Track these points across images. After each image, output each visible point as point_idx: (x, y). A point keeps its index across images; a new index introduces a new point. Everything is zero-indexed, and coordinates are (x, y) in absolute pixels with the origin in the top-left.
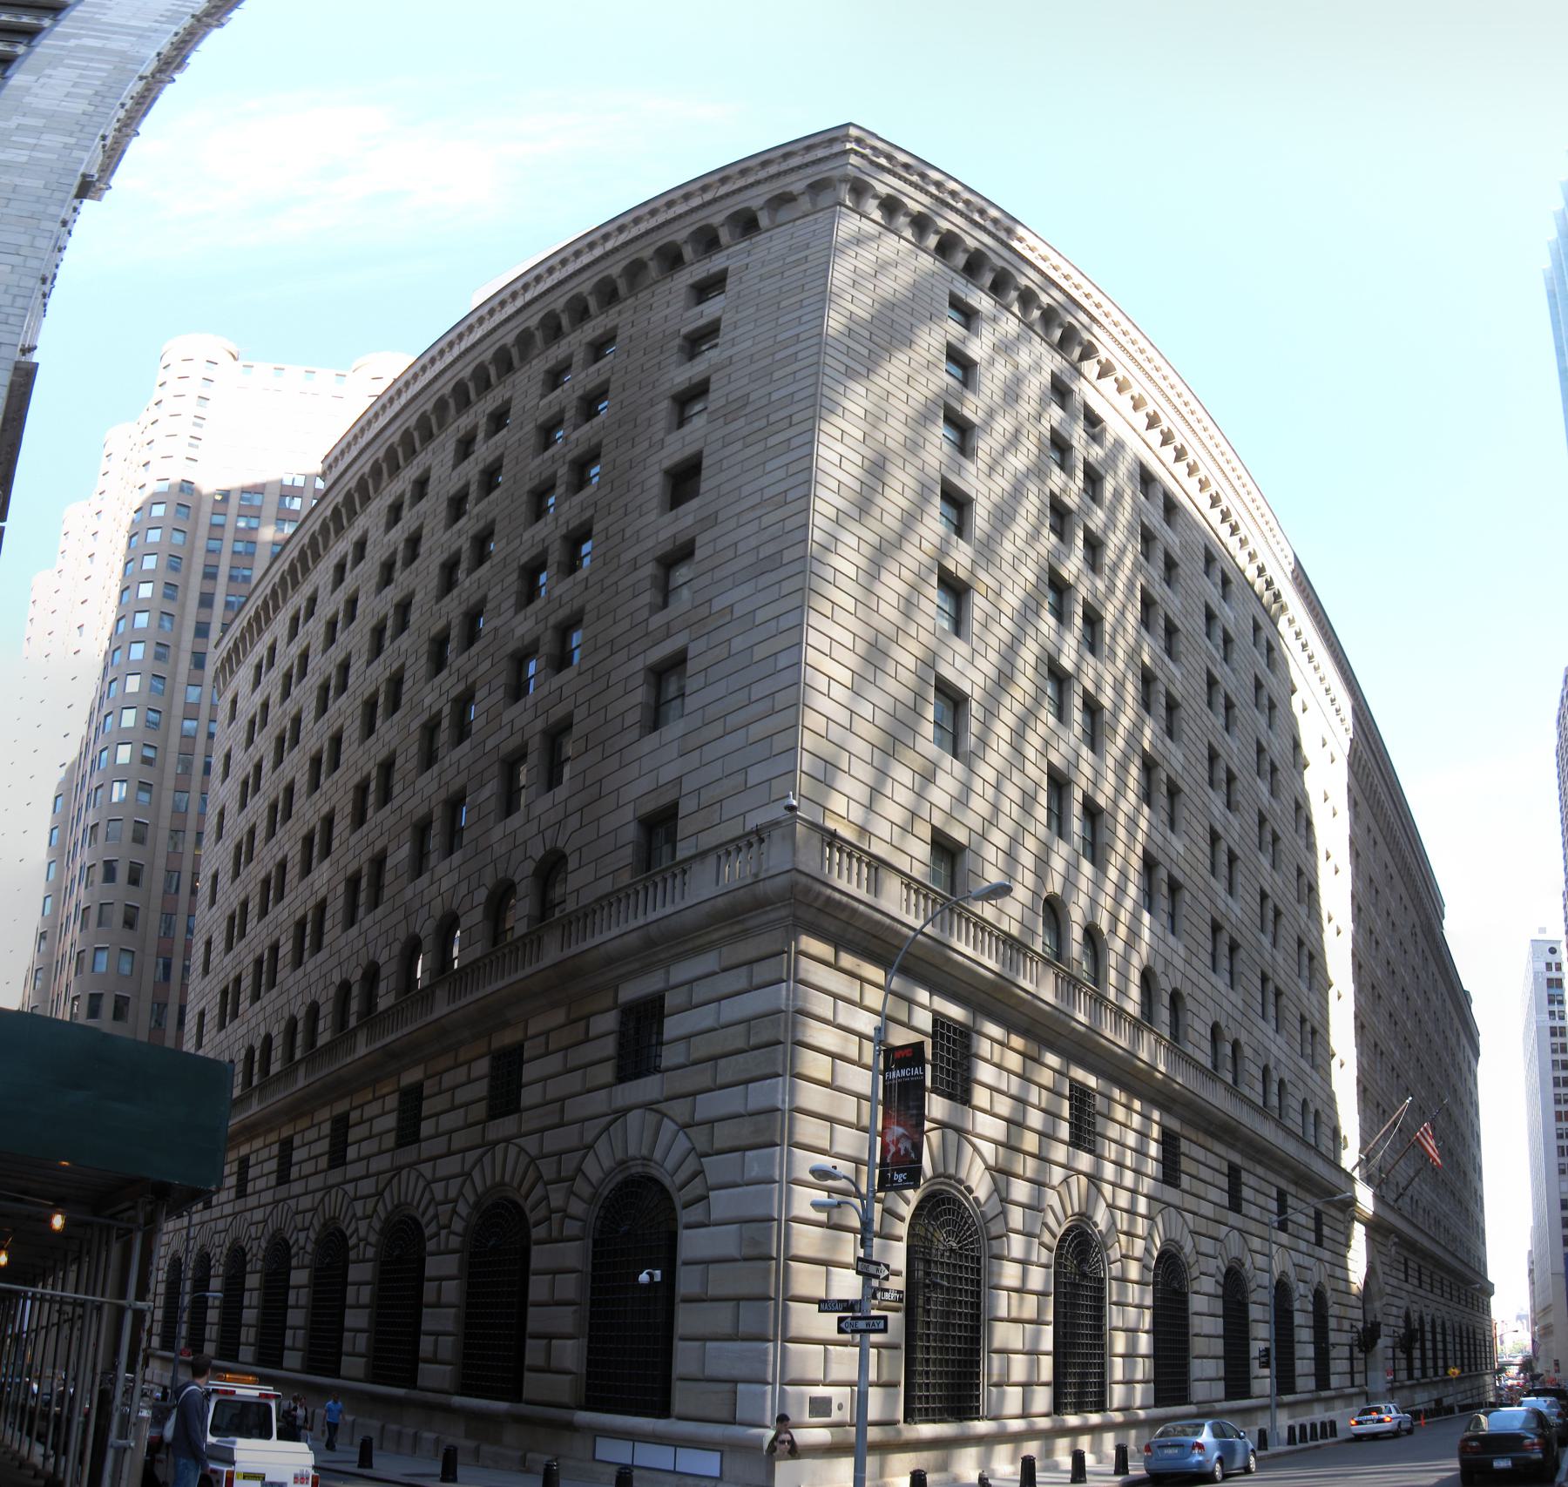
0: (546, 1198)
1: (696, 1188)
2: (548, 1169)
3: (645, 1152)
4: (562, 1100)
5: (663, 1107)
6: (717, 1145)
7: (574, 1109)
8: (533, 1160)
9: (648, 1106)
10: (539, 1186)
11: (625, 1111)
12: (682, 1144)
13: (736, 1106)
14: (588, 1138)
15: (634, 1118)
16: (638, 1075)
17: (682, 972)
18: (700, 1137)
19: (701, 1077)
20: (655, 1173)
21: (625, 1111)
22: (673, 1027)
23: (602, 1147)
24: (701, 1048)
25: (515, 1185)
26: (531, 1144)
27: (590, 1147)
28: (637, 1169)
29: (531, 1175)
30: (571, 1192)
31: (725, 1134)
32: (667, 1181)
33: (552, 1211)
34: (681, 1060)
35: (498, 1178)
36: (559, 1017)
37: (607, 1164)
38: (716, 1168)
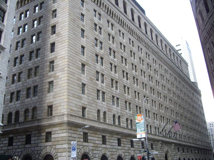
0: (35, 156)
1: (56, 157)
2: (35, 152)
3: (50, 151)
4: (38, 143)
5: (52, 146)
6: (59, 152)
7: (39, 145)
8: (33, 151)
9: (50, 146)
10: (34, 155)
11: (47, 146)
12: (54, 151)
13: (61, 148)
14: (42, 149)
15: (48, 147)
16: (48, 142)
17: (54, 129)
18: (57, 150)
19: (56, 143)
20: (51, 154)
21: (47, 146)
22: (53, 136)
23: (44, 150)
24: (56, 139)
25: (30, 154)
26: (33, 149)
27: (42, 150)
28: (48, 154)
29: (33, 153)
30: (39, 156)
31: (60, 150)
32: (53, 156)
33: (36, 158)
34: (54, 141)
35: (27, 153)
36: (37, 132)
37: (45, 152)
38: (59, 154)
